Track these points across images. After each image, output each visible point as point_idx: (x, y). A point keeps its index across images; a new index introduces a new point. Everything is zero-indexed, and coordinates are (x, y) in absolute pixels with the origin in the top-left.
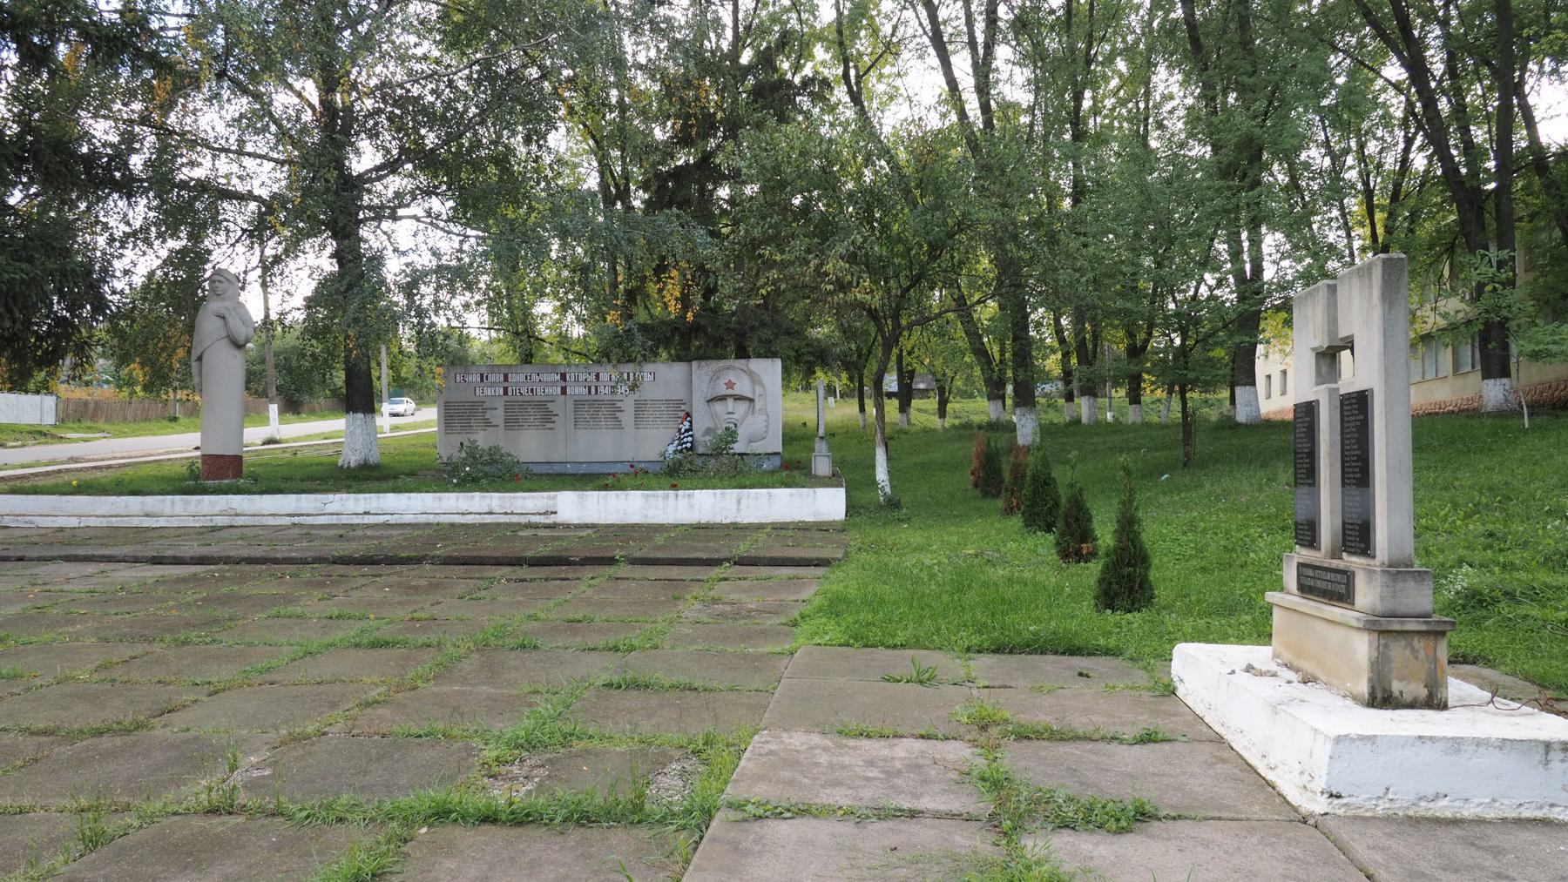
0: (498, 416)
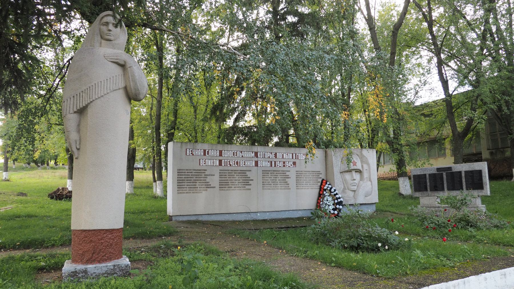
0: (215, 181)
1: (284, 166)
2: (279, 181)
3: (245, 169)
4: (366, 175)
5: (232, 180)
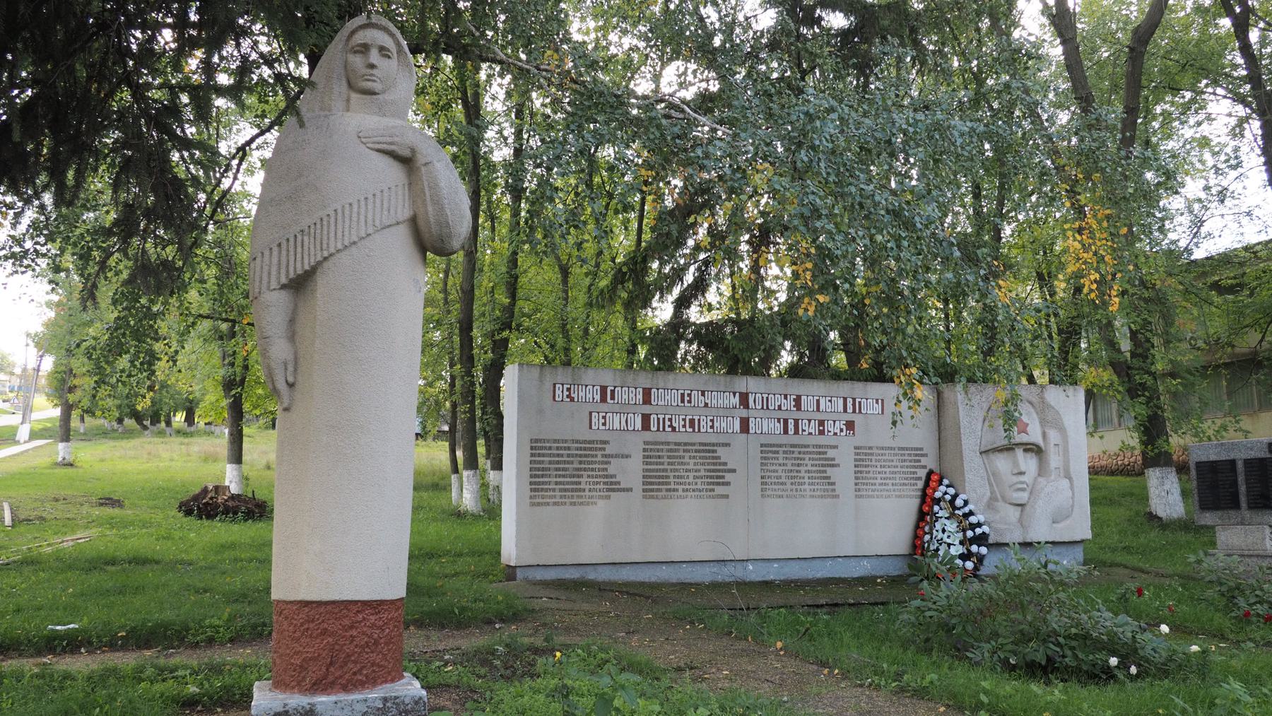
0: (631, 471)
1: (822, 433)
2: (807, 475)
3: (713, 439)
4: (1054, 460)
5: (676, 470)
